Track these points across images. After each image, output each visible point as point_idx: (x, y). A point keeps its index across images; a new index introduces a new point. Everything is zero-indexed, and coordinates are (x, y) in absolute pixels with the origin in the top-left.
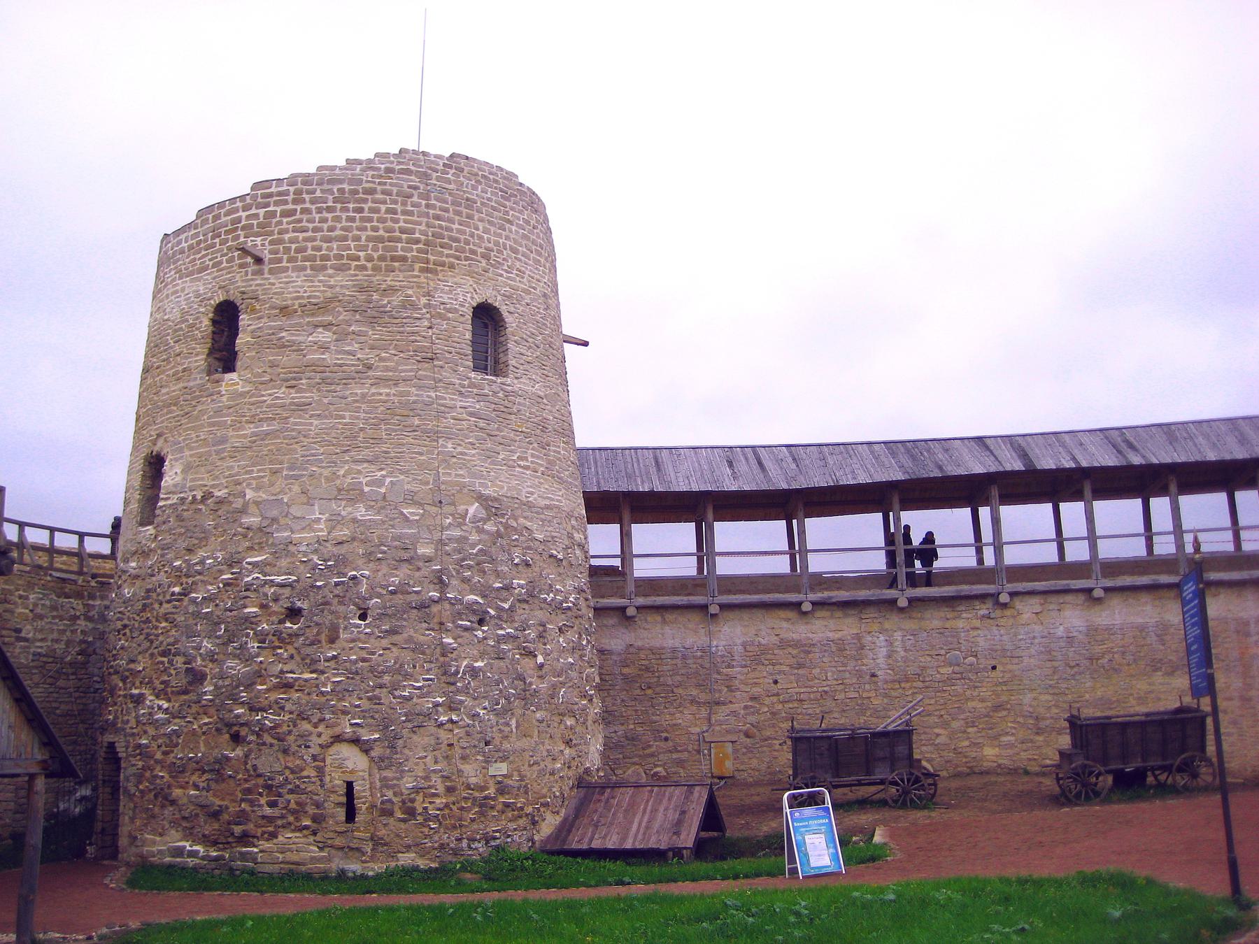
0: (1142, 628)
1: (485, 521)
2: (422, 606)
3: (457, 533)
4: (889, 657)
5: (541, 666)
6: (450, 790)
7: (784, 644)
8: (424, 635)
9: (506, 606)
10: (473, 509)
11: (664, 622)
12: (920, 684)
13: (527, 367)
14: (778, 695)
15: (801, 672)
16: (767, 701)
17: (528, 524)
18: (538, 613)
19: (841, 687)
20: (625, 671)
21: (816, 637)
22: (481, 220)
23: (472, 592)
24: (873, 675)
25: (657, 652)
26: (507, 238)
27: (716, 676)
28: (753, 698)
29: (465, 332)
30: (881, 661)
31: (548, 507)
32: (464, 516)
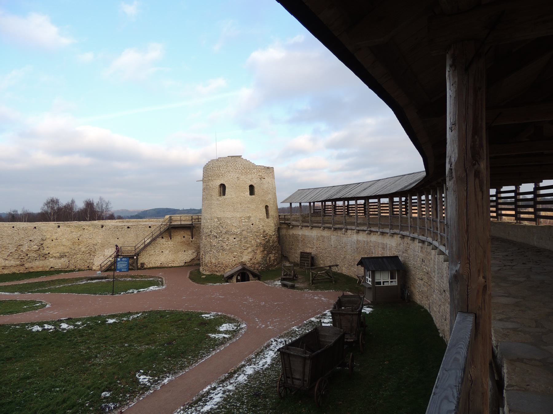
0: (364, 242)
1: (218, 222)
2: (209, 235)
3: (213, 224)
4: (334, 241)
5: (227, 245)
6: (211, 263)
7: (322, 236)
8: (209, 240)
9: (220, 235)
10: (216, 220)
11: (306, 230)
12: (336, 249)
13: (231, 192)
14: (320, 247)
15: (323, 243)
16: (319, 248)
17: (227, 221)
18: (227, 236)
19: (328, 247)
20: (301, 239)
21: (325, 235)
22: (222, 169)
23: (215, 233)
24: (332, 245)
25: (305, 235)
26: (227, 170)
27: (312, 242)
28: (317, 248)
29: (217, 190)
30: (333, 242)
31: (232, 217)
32: (215, 221)
